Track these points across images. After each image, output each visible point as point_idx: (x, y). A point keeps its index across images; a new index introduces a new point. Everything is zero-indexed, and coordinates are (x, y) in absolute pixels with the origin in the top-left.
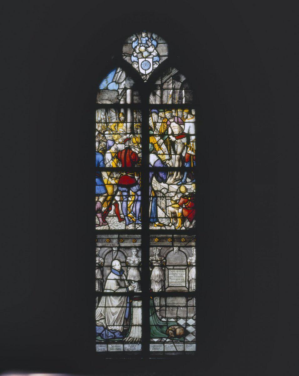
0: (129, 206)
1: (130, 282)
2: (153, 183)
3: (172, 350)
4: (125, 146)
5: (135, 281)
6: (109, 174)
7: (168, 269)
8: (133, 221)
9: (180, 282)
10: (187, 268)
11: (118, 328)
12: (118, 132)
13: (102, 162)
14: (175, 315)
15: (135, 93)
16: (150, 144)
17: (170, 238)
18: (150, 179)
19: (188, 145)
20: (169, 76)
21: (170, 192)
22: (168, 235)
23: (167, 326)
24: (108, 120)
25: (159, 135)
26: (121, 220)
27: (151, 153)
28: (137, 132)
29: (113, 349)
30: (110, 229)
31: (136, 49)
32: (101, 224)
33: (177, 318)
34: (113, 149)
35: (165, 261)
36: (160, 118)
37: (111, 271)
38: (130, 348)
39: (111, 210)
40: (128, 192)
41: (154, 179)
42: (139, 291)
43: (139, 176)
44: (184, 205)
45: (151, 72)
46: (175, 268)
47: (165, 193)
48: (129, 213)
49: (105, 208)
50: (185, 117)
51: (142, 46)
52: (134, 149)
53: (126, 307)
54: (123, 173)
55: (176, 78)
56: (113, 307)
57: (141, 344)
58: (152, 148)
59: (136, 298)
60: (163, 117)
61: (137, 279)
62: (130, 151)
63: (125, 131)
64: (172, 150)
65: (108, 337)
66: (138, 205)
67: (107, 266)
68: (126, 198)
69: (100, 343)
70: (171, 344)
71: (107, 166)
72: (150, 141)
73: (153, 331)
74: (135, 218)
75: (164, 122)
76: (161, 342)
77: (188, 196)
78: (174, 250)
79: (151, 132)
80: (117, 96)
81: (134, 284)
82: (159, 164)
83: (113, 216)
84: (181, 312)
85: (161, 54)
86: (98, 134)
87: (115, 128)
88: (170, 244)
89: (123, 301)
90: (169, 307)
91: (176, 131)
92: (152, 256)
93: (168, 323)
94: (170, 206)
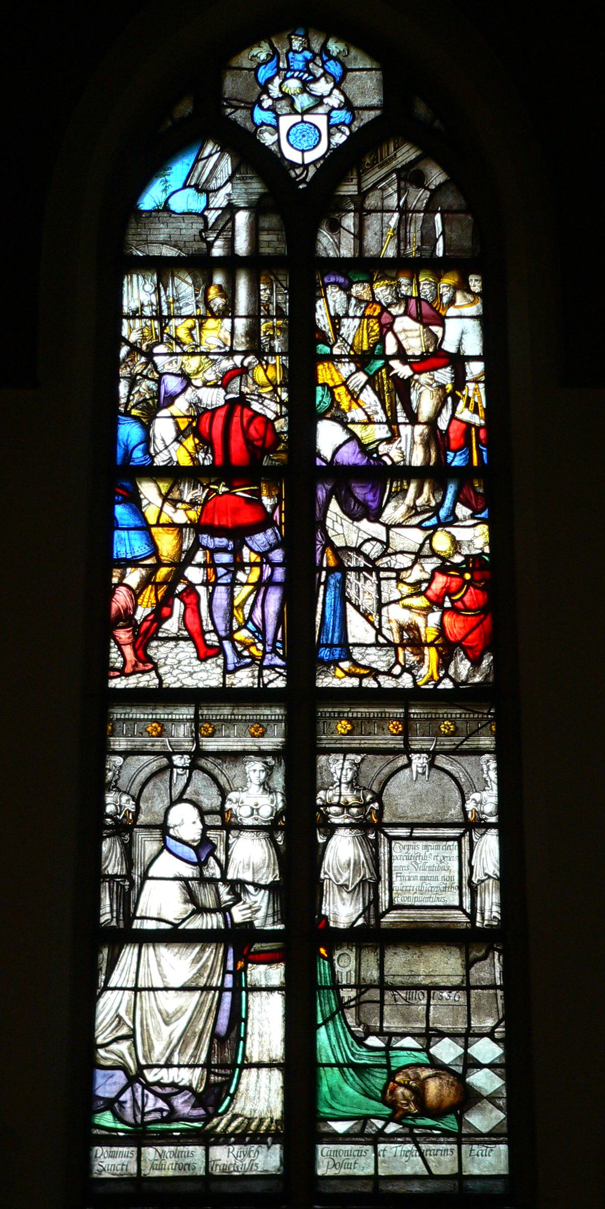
0: (236, 603)
1: (238, 888)
2: (329, 523)
3: (408, 1171)
4: (227, 393)
5: (258, 886)
6: (164, 491)
7: (391, 839)
8: (252, 656)
10: (463, 835)
11: (185, 1077)
12: (202, 349)
13: (141, 446)
14: (421, 1022)
15: (265, 223)
16: (319, 389)
17: (396, 719)
18: (318, 508)
19: (458, 393)
21: (396, 553)
22: (387, 710)
23: (388, 1066)
24: (164, 307)
25: (352, 359)
26: (205, 653)
27: (322, 417)
28: (272, 348)
30: (164, 686)
31: (270, 86)
32: (129, 669)
33: (430, 1035)
34: (181, 406)
36: (353, 301)
37: (165, 847)
39: (170, 615)
40: (237, 553)
41: (334, 506)
42: (274, 923)
43: (279, 496)
44: (447, 599)
45: (322, 157)
46: (418, 832)
47: (373, 555)
48: (239, 630)
49: (149, 611)
50: (445, 300)
51: (292, 77)
52: (262, 404)
53: (222, 989)
56: (166, 989)
57: (278, 1146)
58: (327, 401)
60: (364, 301)
61: (268, 876)
63: (229, 344)
64: (399, 407)
65: (144, 1114)
66: (274, 599)
67: (148, 827)
68: (225, 574)
69: (111, 1139)
71: (159, 461)
72: (320, 377)
74: (260, 646)
75: (370, 317)
76: (361, 1134)
77: (464, 566)
78: (414, 766)
79: (323, 349)
80: (200, 232)
82: (350, 456)
83: (177, 639)
84: (444, 1010)
86: (128, 354)
87: (192, 336)
89: (210, 963)
90: (394, 988)
91: (415, 344)
92: (326, 790)
93: (392, 1053)
94: (396, 602)
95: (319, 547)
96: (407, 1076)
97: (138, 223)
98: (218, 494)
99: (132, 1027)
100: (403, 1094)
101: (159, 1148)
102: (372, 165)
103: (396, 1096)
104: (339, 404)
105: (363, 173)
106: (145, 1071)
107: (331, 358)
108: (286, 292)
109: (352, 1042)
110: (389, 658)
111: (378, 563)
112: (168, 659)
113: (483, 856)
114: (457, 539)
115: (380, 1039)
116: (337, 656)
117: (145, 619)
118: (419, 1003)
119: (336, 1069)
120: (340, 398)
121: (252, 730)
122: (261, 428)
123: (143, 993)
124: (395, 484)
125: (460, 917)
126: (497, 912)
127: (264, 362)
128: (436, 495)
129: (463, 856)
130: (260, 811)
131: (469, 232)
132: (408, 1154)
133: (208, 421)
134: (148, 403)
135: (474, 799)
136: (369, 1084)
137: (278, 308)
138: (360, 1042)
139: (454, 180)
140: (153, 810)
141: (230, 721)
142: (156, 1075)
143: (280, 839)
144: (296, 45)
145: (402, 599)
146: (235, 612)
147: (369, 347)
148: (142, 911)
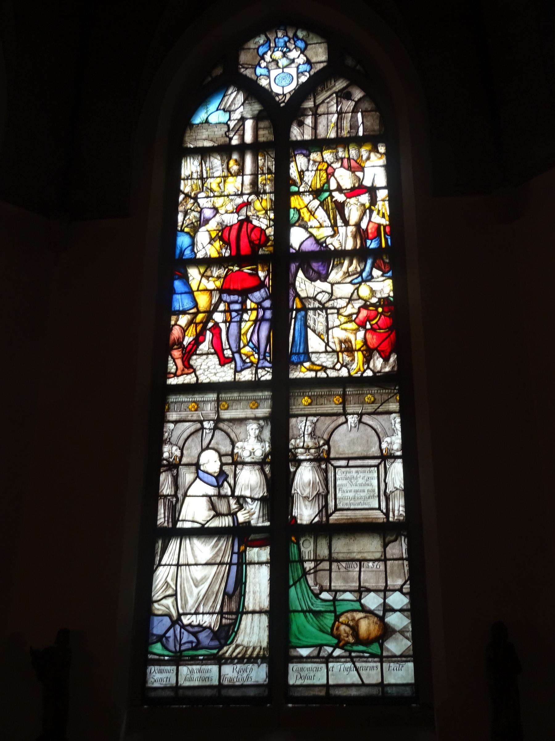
0: (243, 332)
1: (241, 501)
2: (297, 284)
3: (349, 681)
4: (239, 216)
5: (253, 499)
7: (335, 468)
8: (251, 362)
9: (365, 498)
10: (380, 463)
11: (208, 620)
12: (226, 193)
14: (356, 582)
15: (261, 125)
16: (292, 211)
19: (373, 207)
20: (329, 93)
21: (337, 299)
23: (335, 611)
26: (224, 361)
27: (294, 225)
29: (191, 679)
30: (199, 381)
32: (179, 372)
33: (361, 591)
34: (213, 225)
35: (326, 447)
37: (198, 477)
38: (235, 674)
40: (243, 303)
41: (300, 274)
42: (263, 522)
43: (268, 271)
44: (368, 323)
46: (352, 463)
47: (323, 301)
48: (244, 346)
49: (191, 339)
50: (364, 158)
52: (259, 220)
53: (230, 564)
54: (233, 266)
55: (344, 95)
56: (196, 564)
58: (296, 216)
59: (252, 540)
61: (259, 494)
62: (250, 226)
63: (240, 189)
64: (338, 217)
66: (265, 328)
67: (188, 465)
68: (236, 316)
69: (160, 662)
70: (346, 662)
71: (200, 255)
73: (298, 628)
74: (256, 356)
75: (320, 170)
76: (318, 656)
79: (294, 189)
80: (226, 133)
81: (251, 507)
82: (310, 246)
83: (207, 354)
84: (370, 574)
85: (314, 60)
86: (183, 199)
87: (220, 187)
88: (339, 409)
89: (223, 548)
93: (337, 603)
95: (291, 298)
96: (347, 617)
97: (191, 130)
98: (233, 271)
99: (175, 589)
100: (345, 630)
101: (190, 667)
102: (322, 91)
103: (340, 631)
104: (303, 218)
105: (317, 95)
106: (182, 617)
107: (298, 193)
108: (273, 159)
109: (312, 597)
110: (333, 359)
111: (326, 305)
112: (202, 366)
113: (393, 476)
114: (374, 289)
115: (329, 594)
116: (302, 359)
117: (190, 344)
118: (354, 570)
119: (302, 614)
120: (303, 214)
121: (251, 405)
122: (258, 235)
123: (182, 567)
124: (336, 260)
125: (379, 516)
126: (402, 511)
127: (260, 198)
128: (361, 265)
129: (380, 476)
130: (255, 453)
131: (378, 122)
132: (348, 670)
133: (227, 232)
134: (194, 224)
135: (387, 441)
136: (322, 623)
137: (269, 169)
138: (317, 596)
139: (368, 95)
140: (191, 455)
141: (238, 400)
142: (189, 619)
143: (267, 469)
144: (280, 34)
145: (341, 325)
146: (242, 337)
147: (321, 185)
148: (183, 516)
